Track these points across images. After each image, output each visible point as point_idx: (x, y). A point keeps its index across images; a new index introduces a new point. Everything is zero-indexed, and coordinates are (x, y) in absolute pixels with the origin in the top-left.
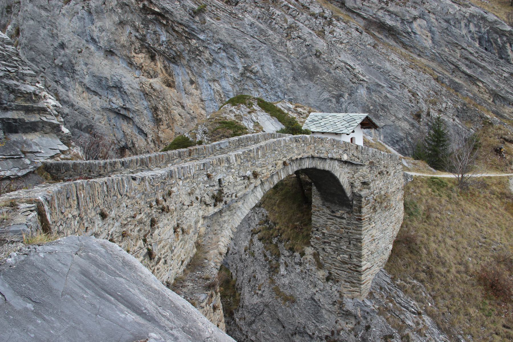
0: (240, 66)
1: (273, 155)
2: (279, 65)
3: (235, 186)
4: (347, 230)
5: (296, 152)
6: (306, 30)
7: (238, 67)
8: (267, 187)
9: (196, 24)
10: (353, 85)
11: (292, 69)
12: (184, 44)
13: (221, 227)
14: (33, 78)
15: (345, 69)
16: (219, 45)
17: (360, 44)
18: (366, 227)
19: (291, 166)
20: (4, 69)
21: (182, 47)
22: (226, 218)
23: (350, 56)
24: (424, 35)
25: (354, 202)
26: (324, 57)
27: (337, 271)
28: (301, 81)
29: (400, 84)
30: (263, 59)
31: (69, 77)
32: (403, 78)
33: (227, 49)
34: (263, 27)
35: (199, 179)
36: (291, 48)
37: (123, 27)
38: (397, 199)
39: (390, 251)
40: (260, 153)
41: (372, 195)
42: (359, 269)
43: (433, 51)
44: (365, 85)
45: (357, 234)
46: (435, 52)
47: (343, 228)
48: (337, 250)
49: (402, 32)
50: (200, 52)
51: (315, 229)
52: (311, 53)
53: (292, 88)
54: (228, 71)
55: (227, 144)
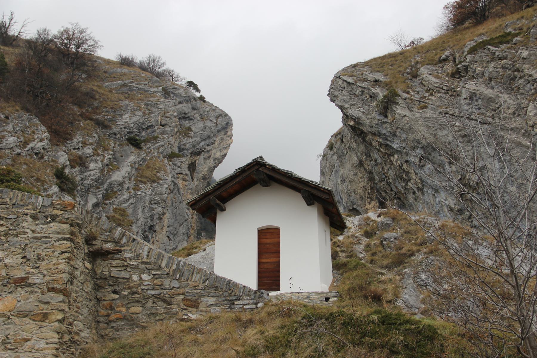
33: (430, 154)
54: (442, 196)
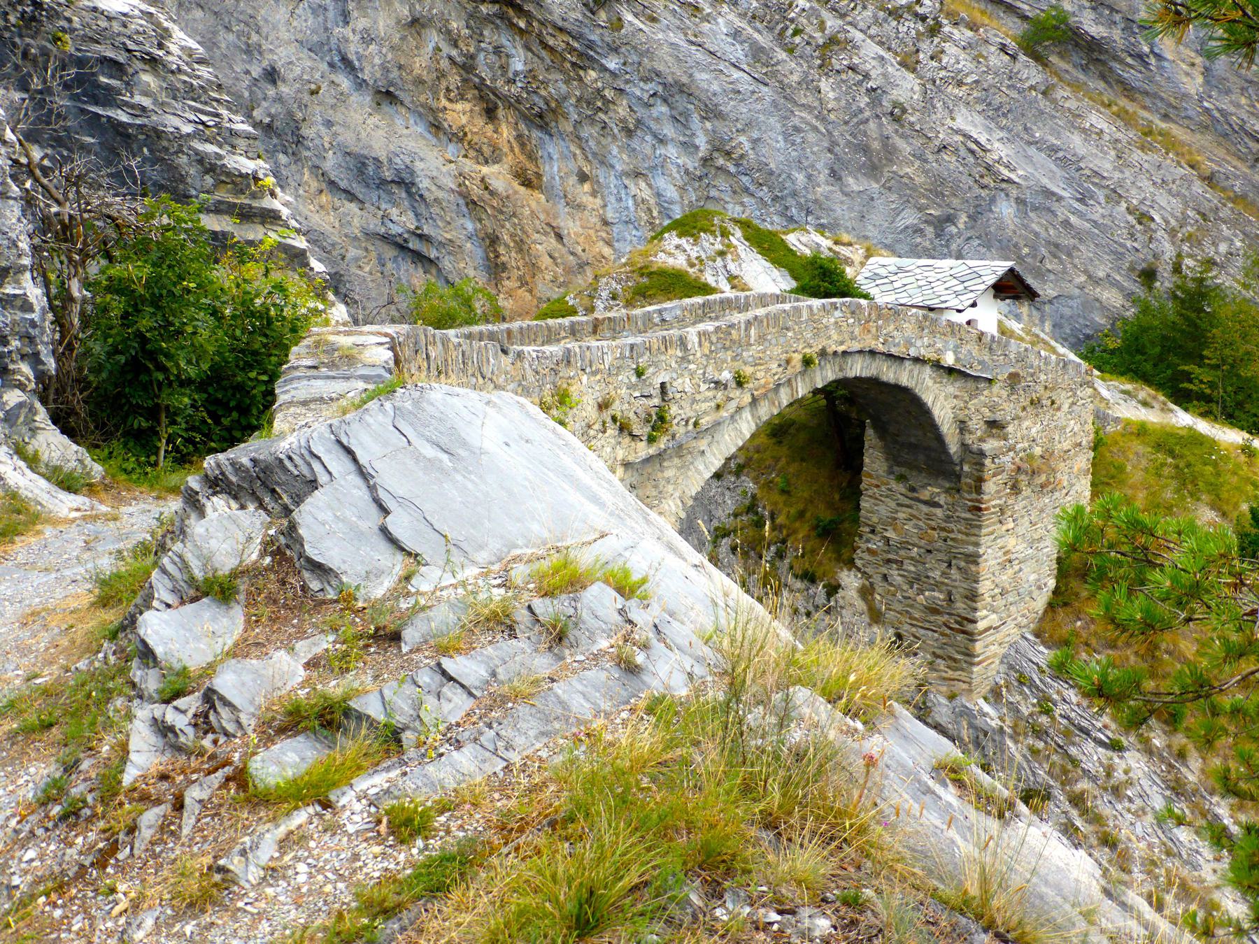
0: (701, 141)
1: (782, 340)
2: (799, 140)
3: (694, 401)
4: (944, 534)
5: (835, 337)
6: (871, 49)
7: (697, 142)
8: (766, 411)
9: (599, 31)
10: (984, 193)
11: (830, 151)
12: (567, 82)
13: (660, 492)
14: (251, 142)
15: (963, 152)
16: (651, 87)
17: (1009, 87)
18: (990, 529)
19: (822, 368)
20: (192, 117)
21: (563, 88)
22: (670, 473)
23: (978, 119)
24: (1183, 61)
25: (966, 468)
26: (912, 119)
27: (914, 629)
28: (851, 180)
29: (1107, 192)
30: (758, 124)
31: (285, 153)
32: (1117, 175)
34: (764, 40)
35: (620, 378)
36: (831, 95)
37: (419, 34)
38: (1075, 469)
39: (1050, 594)
40: (752, 331)
41: (1011, 454)
42: (970, 627)
43: (1206, 104)
44: (1014, 192)
45: (968, 543)
46: (1212, 107)
47: (934, 529)
48: (917, 580)
49: (1124, 55)
50: (607, 102)
51: (867, 529)
52: (879, 111)
53: (827, 198)
54: (671, 151)
55: (679, 312)
